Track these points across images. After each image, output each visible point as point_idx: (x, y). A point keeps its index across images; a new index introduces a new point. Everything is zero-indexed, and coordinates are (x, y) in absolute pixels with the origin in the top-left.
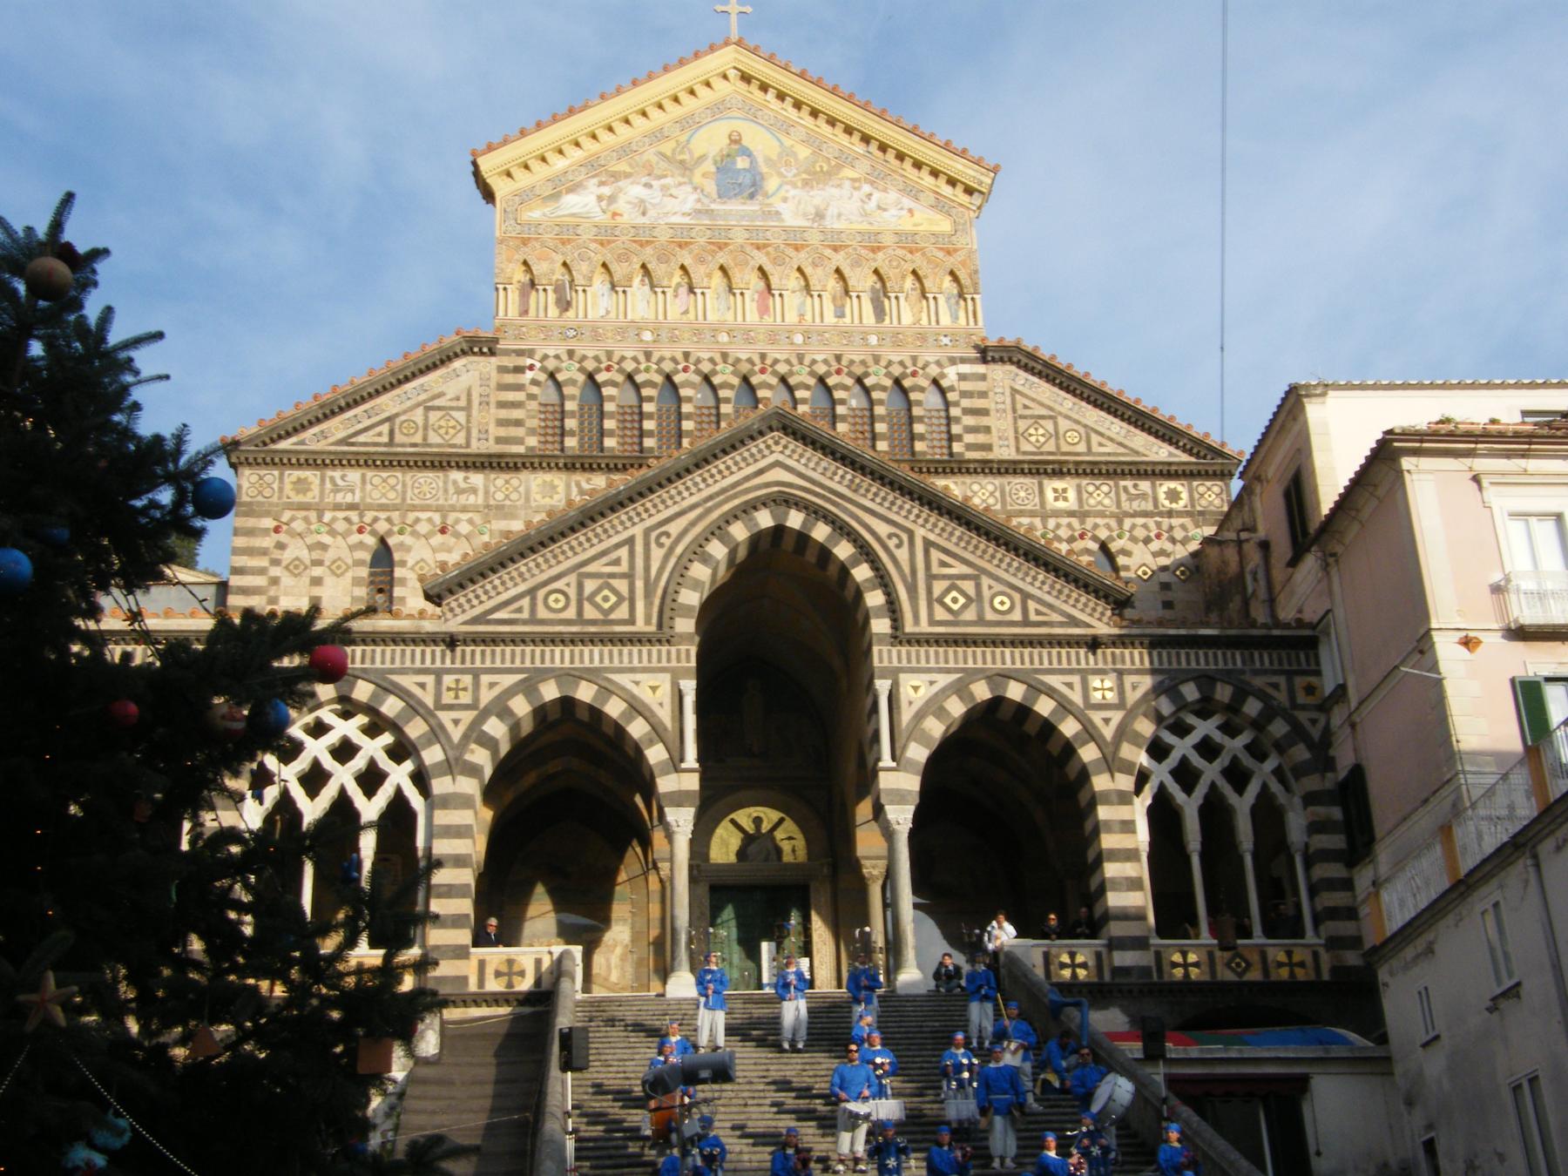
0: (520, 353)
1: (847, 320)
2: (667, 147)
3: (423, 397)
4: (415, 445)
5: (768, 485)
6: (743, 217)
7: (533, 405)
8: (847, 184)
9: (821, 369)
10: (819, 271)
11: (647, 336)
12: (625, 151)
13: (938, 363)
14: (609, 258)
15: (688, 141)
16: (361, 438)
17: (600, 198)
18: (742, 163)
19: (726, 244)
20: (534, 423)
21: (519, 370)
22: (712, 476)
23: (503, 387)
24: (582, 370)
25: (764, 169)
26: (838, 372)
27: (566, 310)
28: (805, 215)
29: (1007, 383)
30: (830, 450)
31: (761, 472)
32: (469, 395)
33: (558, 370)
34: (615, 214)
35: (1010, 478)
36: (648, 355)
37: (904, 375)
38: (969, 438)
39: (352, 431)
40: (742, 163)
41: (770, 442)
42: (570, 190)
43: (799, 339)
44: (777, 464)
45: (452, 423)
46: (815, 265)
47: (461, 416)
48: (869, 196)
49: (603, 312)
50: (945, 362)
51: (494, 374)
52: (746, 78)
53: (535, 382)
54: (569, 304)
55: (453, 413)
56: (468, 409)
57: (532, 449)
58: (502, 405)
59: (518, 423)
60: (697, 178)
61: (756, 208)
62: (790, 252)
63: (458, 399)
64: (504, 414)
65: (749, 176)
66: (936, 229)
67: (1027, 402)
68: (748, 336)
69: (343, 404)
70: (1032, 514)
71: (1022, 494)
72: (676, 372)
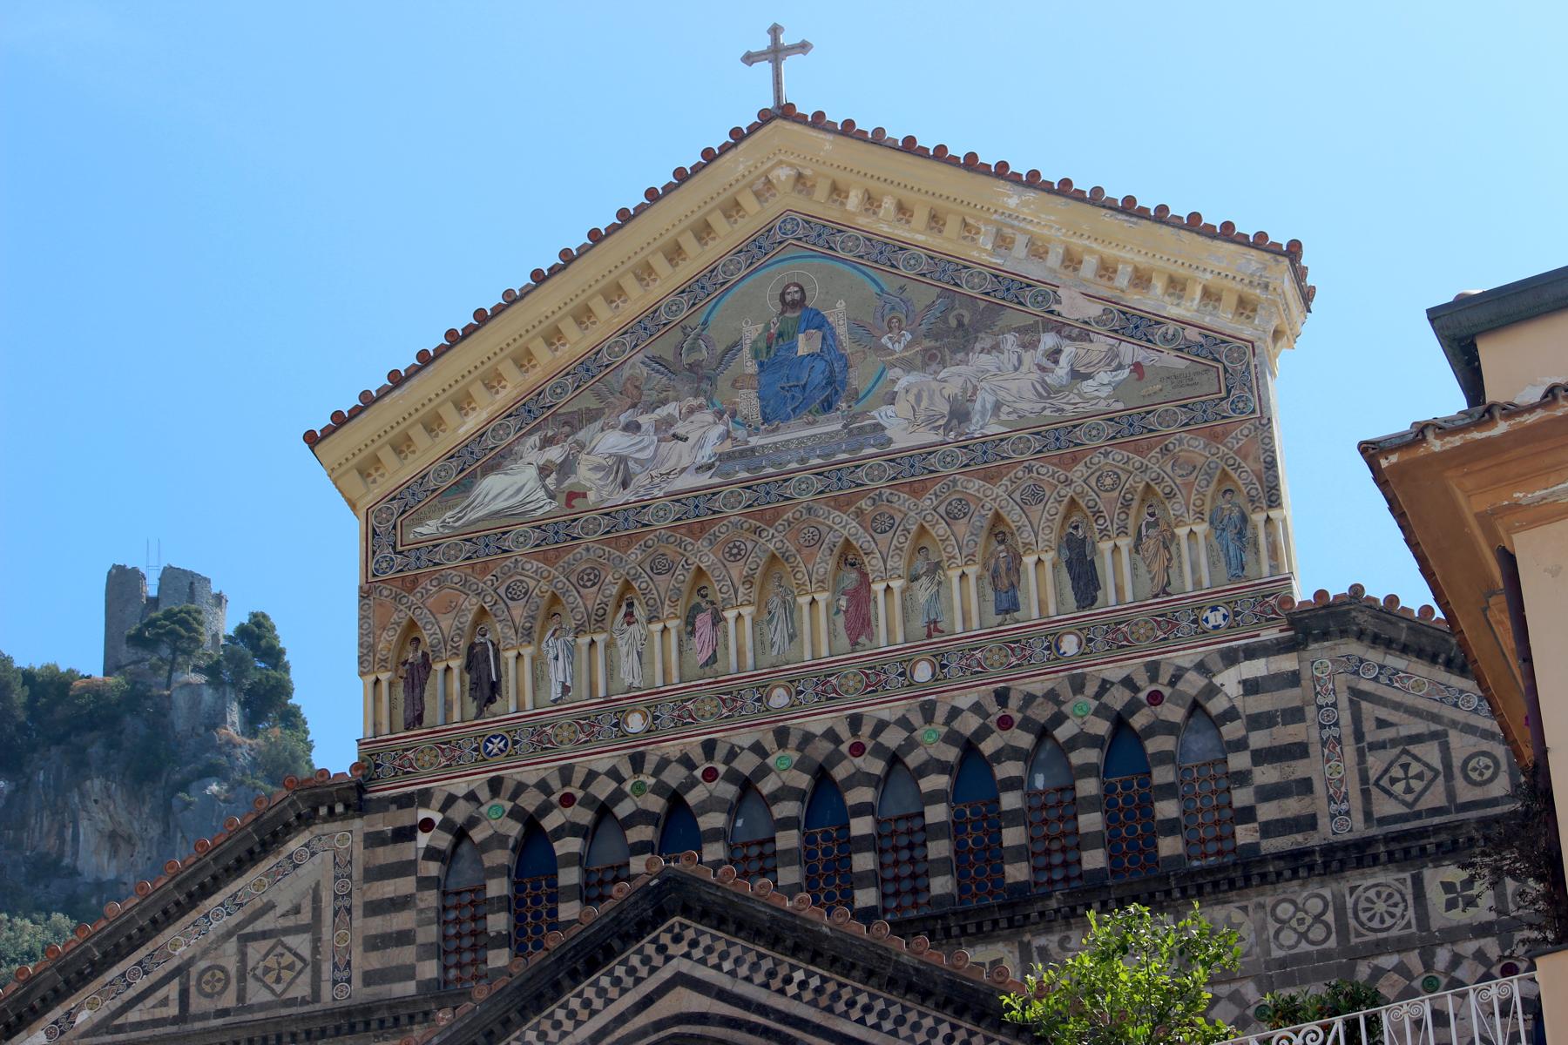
0: (405, 802)
3: (238, 917)
4: (224, 1012)
5: (659, 1025)
7: (431, 898)
8: (1011, 338)
9: (969, 724)
10: (961, 527)
12: (589, 368)
13: (1201, 667)
15: (705, 323)
16: (133, 1016)
17: (544, 471)
19: (778, 513)
20: (430, 934)
21: (405, 834)
23: (375, 874)
26: (1005, 723)
27: (491, 700)
28: (930, 421)
29: (1342, 681)
30: (778, 934)
31: (647, 1002)
32: (316, 899)
33: (473, 822)
34: (572, 496)
35: (1354, 878)
36: (637, 762)
37: (1133, 707)
38: (1267, 812)
39: (118, 1003)
40: (805, 345)
41: (666, 939)
42: (488, 469)
43: (923, 672)
44: (681, 980)
45: (288, 958)
46: (951, 517)
47: (301, 943)
48: (1054, 355)
49: (556, 691)
50: (1215, 663)
53: (431, 853)
55: (290, 940)
56: (314, 928)
59: (403, 938)
61: (838, 426)
62: (903, 501)
63: (297, 910)
64: (378, 925)
65: (820, 365)
67: (1383, 713)
68: (821, 684)
69: (97, 955)
70: (1401, 945)
71: (1381, 907)
72: (691, 784)
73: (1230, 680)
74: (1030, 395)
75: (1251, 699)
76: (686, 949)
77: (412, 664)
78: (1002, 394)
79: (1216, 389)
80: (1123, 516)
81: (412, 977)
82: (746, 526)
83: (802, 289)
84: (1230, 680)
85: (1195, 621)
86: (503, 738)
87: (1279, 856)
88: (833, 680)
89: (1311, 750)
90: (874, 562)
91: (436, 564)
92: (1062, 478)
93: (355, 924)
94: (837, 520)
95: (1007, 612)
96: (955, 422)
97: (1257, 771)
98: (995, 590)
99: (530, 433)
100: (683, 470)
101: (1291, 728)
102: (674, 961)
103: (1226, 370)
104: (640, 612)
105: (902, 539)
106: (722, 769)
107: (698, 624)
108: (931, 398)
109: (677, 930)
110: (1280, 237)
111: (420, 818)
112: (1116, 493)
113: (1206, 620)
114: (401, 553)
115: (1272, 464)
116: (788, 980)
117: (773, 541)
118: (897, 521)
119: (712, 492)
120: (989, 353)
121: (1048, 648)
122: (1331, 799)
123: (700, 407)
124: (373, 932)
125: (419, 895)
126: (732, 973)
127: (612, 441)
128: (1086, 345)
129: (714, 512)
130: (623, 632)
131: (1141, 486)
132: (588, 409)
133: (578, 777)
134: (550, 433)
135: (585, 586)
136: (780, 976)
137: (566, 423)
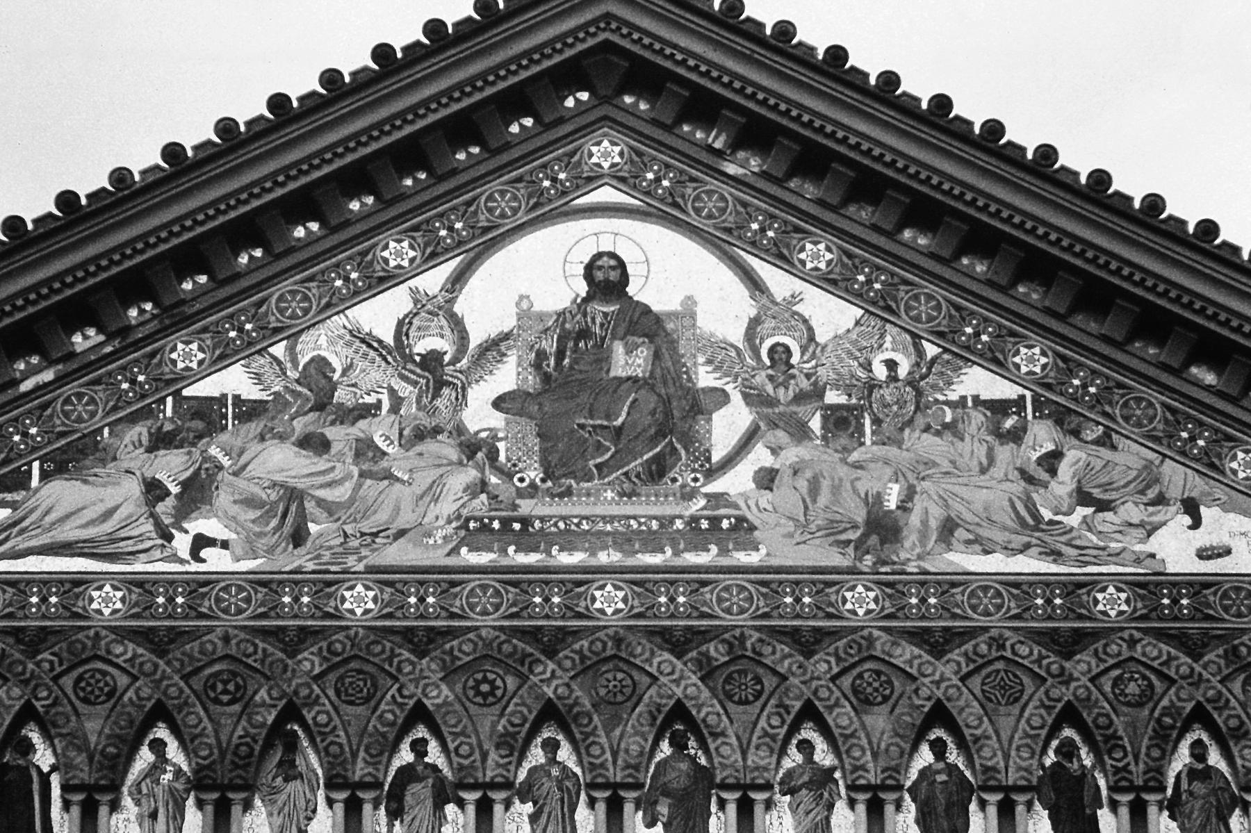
2: (379, 314)
8: (978, 418)
10: (878, 721)
17: (154, 491)
18: (628, 361)
25: (705, 378)
28: (832, 530)
34: (201, 542)
48: (1051, 461)
52: (645, 77)
62: (781, 656)
78: (957, 506)
80: (1156, 753)
82: (506, 648)
83: (622, 265)
96: (874, 540)
99: (133, 419)
100: (401, 533)
105: (775, 721)
107: (408, 799)
108: (836, 489)
117: (551, 680)
119: (448, 579)
120: (938, 433)
123: (437, 431)
127: (280, 461)
128: (1105, 453)
129: (453, 616)
131: (1189, 706)
132: (237, 398)
134: (168, 427)
135: (216, 701)
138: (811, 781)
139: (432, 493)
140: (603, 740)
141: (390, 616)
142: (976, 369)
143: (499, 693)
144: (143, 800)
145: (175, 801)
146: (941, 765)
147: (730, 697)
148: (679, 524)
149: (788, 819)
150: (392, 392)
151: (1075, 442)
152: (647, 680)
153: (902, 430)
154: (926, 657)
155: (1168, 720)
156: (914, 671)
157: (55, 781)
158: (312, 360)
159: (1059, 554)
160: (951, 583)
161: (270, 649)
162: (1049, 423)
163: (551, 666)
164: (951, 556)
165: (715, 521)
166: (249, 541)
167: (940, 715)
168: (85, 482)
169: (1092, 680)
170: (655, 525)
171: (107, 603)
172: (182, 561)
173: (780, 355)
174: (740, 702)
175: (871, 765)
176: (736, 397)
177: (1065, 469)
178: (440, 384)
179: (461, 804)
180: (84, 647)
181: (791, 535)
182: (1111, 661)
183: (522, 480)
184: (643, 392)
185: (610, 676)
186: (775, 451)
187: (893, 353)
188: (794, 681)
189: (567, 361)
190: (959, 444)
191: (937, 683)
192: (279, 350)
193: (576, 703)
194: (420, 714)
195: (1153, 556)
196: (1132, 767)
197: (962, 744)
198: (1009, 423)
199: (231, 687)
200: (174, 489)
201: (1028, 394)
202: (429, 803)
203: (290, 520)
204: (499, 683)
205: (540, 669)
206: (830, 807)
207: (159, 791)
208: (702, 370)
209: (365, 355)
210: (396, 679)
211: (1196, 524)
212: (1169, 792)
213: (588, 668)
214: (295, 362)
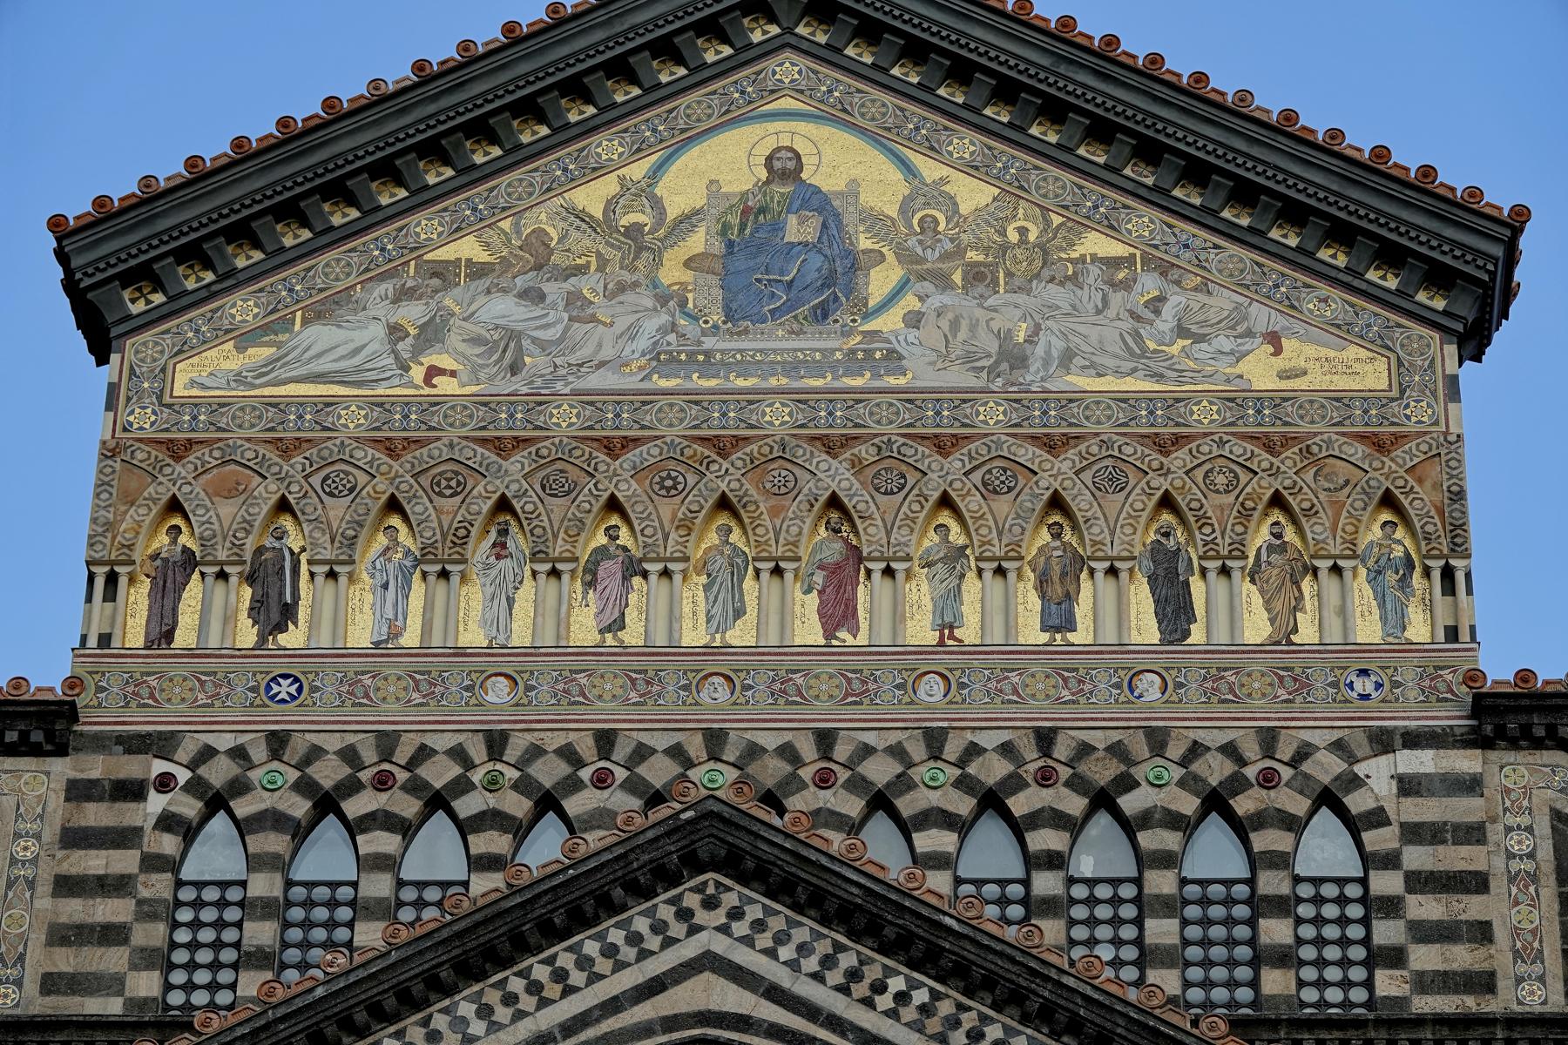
1: (1081, 636)
2: (591, 197)
6: (792, 369)
8: (1094, 270)
9: (993, 770)
10: (1002, 505)
11: (498, 693)
13: (1338, 747)
14: (406, 488)
17: (396, 332)
21: (131, 791)
22: (510, 999)
23: (75, 838)
24: (305, 786)
26: (1045, 778)
27: (281, 628)
28: (969, 358)
31: (655, 987)
33: (239, 787)
34: (433, 372)
37: (1237, 784)
38: (1425, 957)
40: (797, 229)
41: (692, 901)
42: (316, 315)
44: (709, 962)
51: (56, 802)
53: (167, 822)
54: (288, 613)
57: (143, 1003)
58: (67, 886)
59: (112, 934)
60: (672, 272)
64: (75, 910)
66: (1342, 383)
73: (1379, 774)
74: (1117, 349)
75: (1408, 802)
76: (723, 920)
77: (166, 560)
79: (1385, 386)
80: (1239, 529)
81: (120, 993)
82: (688, 452)
83: (798, 157)
84: (1379, 774)
85: (1335, 685)
86: (296, 680)
87: (1440, 1020)
88: (798, 679)
89: (1493, 884)
90: (871, 530)
91: (220, 429)
92: (1155, 465)
93: (38, 904)
94: (823, 466)
95: (1058, 629)
97: (1412, 900)
98: (1043, 597)
99: (382, 277)
100: (602, 364)
101: (1465, 850)
102: (703, 936)
103: (1400, 363)
104: (518, 542)
105: (916, 507)
106: (621, 774)
107: (601, 574)
108: (973, 328)
109: (711, 890)
110: (1500, 197)
111: (154, 774)
112: (1231, 498)
113: (1351, 686)
114: (169, 406)
115: (1458, 496)
116: (879, 988)
117: (727, 477)
118: (911, 482)
120: (1061, 284)
121: (1118, 686)
122: (1517, 954)
123: (636, 284)
124: (63, 919)
125: (142, 878)
126: (793, 965)
127: (503, 309)
129: (643, 427)
130: (488, 567)
132: (469, 261)
133: (403, 754)
134: (410, 284)
135: (440, 494)
136: (867, 982)
137: (435, 274)
138: (946, 556)
139: (631, 333)
140: (768, 523)
141: (591, 428)
142: (1093, 236)
143: (680, 487)
144: (378, 574)
145: (404, 576)
146: (1058, 543)
147: (877, 490)
148: (838, 355)
149: (925, 587)
150: (599, 254)
151: (1177, 289)
152: (808, 476)
153: (1030, 281)
154: (1046, 456)
155: (1249, 504)
156: (1035, 468)
157: (303, 558)
158: (534, 231)
159: (1162, 376)
160: (1073, 398)
161: (487, 453)
162: (1156, 275)
163: (726, 465)
164: (1068, 378)
165: (869, 353)
166: (474, 371)
167: (1056, 503)
168: (339, 326)
169: (1187, 473)
170: (818, 356)
171: (353, 420)
172: (417, 387)
173: (928, 225)
174: (886, 493)
175: (996, 542)
176: (890, 257)
177: (1168, 311)
178: (640, 249)
179: (645, 575)
180: (332, 451)
181: (933, 363)
182: (1203, 458)
183: (706, 322)
184: (811, 254)
185: (775, 473)
186: (921, 299)
187: (1025, 225)
188: (934, 476)
189: (748, 231)
190: (1079, 292)
191: (1055, 477)
192: (506, 225)
193: (746, 494)
194: (613, 505)
195: (1241, 377)
196: (1219, 540)
197: (1075, 527)
198: (1121, 275)
199: (453, 483)
200: (413, 332)
201: (1138, 253)
202: (619, 575)
203: (509, 354)
204: (681, 479)
205: (716, 467)
206: (962, 576)
207: (390, 567)
208: (862, 236)
209: (578, 228)
210: (593, 476)
211: (1278, 351)
212: (1251, 560)
213: (756, 466)
214: (518, 233)
